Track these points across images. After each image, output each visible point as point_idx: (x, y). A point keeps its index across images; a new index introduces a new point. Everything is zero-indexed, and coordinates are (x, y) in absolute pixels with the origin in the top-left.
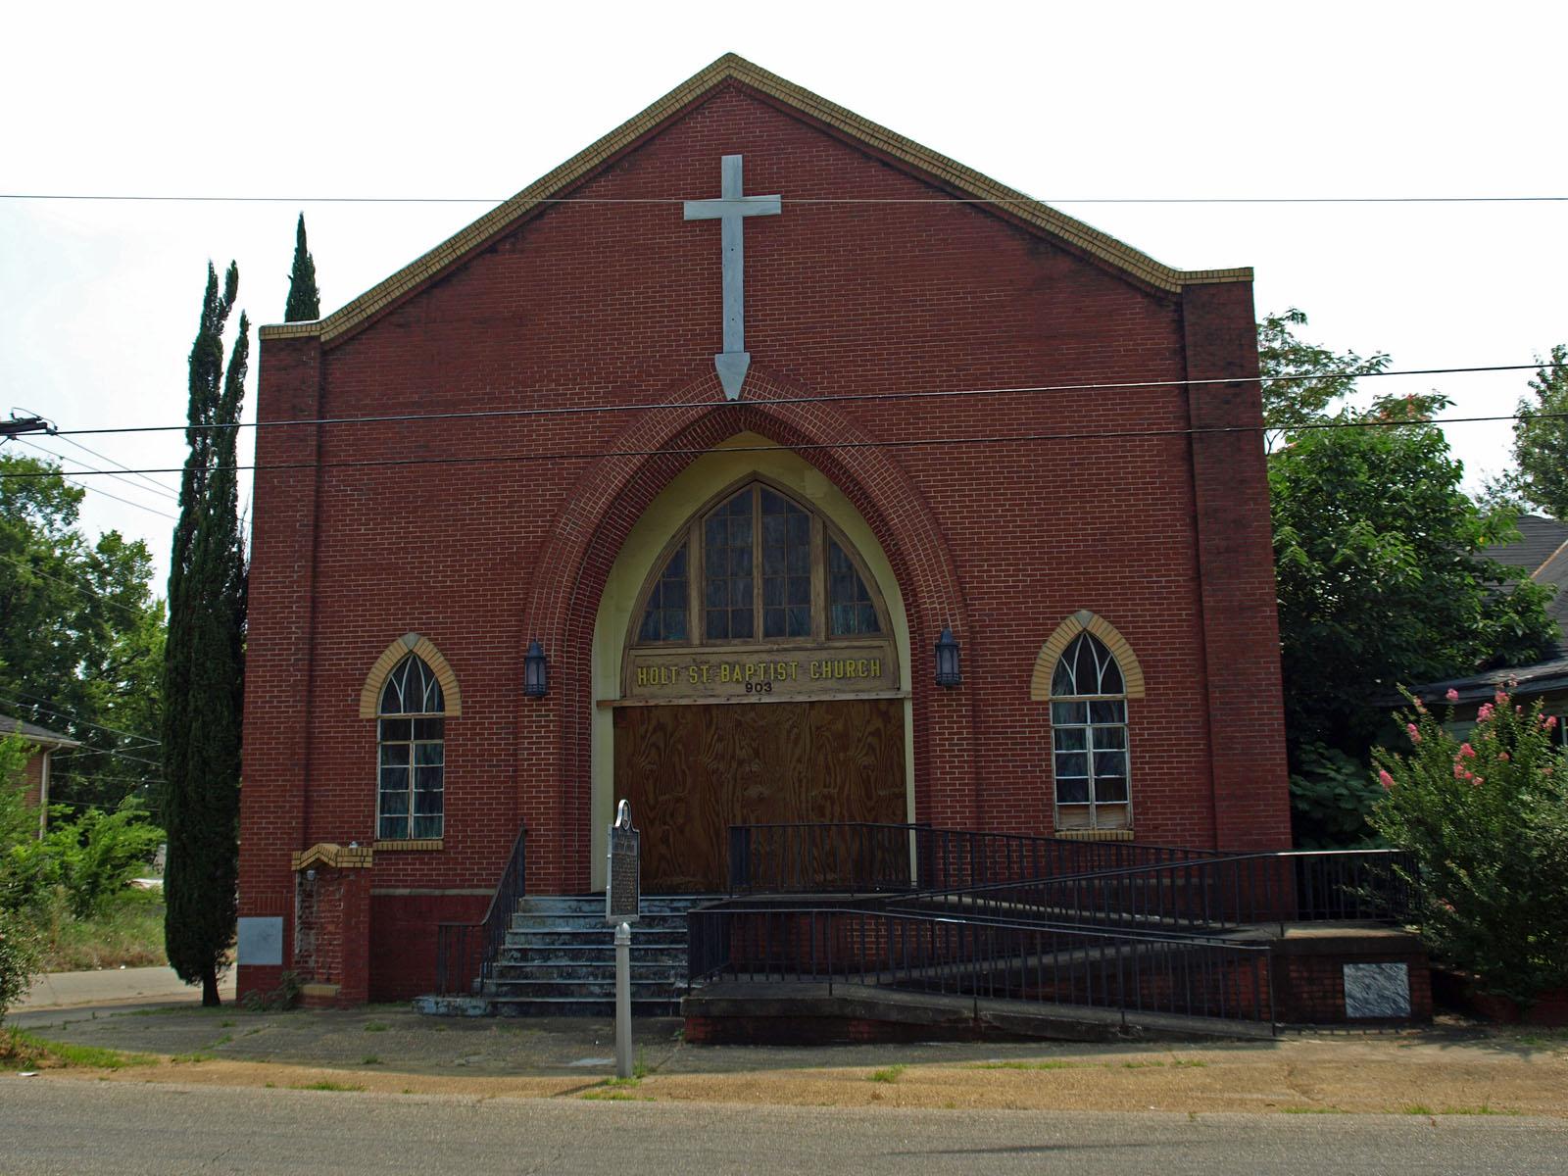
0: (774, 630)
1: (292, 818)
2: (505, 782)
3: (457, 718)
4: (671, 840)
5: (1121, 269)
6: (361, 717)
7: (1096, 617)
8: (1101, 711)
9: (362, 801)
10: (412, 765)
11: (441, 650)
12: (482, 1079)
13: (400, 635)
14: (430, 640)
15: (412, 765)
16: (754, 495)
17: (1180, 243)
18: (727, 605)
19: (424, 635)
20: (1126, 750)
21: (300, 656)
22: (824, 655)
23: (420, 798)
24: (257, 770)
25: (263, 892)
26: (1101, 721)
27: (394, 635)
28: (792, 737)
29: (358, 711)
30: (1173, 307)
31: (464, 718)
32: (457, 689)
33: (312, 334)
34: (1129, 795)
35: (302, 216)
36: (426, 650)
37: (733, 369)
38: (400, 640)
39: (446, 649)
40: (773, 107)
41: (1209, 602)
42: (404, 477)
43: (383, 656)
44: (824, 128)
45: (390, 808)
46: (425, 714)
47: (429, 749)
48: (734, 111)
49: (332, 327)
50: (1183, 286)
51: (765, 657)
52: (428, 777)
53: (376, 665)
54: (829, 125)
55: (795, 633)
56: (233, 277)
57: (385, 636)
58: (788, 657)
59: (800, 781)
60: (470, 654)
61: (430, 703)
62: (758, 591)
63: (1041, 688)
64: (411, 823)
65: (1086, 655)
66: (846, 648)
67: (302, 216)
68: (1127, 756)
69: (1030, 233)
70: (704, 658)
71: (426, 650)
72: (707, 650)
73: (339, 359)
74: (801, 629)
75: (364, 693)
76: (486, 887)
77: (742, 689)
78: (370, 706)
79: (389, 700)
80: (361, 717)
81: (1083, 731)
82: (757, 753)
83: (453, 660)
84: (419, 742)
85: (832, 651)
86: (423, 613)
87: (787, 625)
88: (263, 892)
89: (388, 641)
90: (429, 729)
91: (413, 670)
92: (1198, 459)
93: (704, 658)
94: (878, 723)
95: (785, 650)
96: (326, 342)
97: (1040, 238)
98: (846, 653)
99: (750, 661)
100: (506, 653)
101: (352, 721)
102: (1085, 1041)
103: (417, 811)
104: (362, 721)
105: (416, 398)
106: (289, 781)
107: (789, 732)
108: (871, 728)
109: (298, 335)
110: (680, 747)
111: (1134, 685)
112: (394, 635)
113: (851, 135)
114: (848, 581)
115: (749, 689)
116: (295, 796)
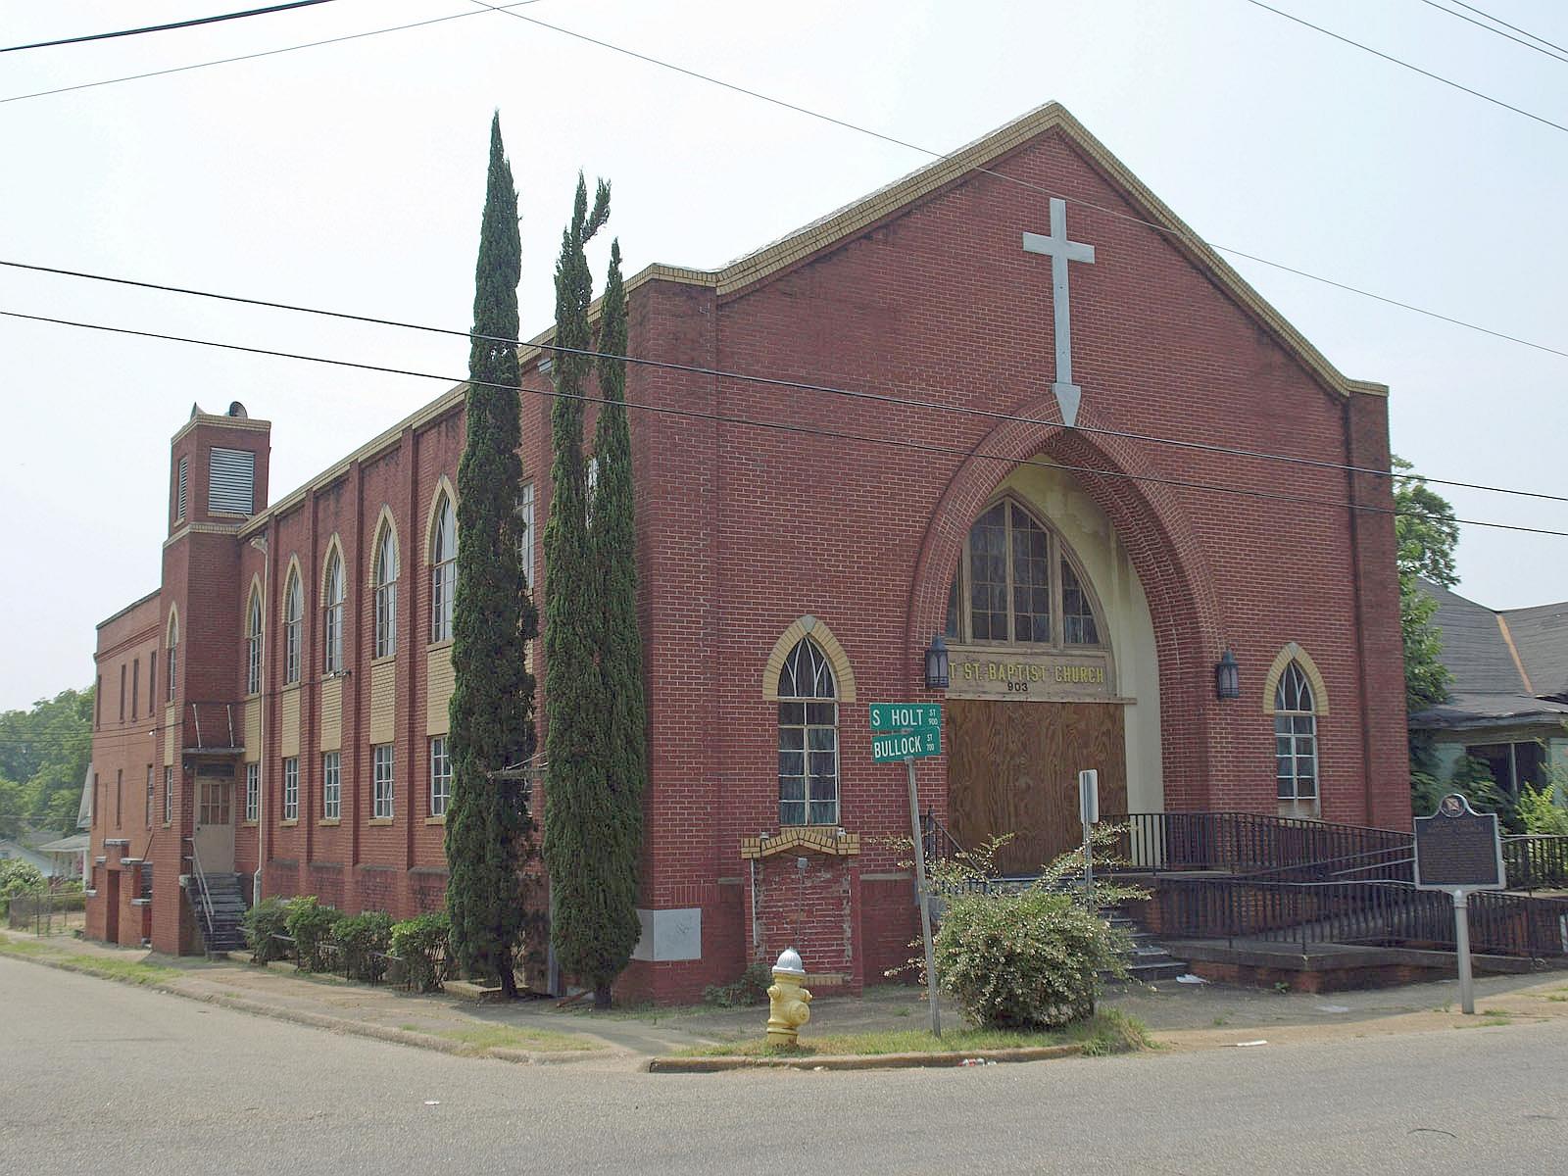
0: (1023, 635)
1: (706, 803)
2: (896, 769)
3: (1326, 717)
4: (961, 827)
5: (1315, 370)
6: (765, 698)
7: (821, 622)
8: (1301, 724)
9: (768, 786)
10: (806, 751)
11: (836, 635)
12: (1381, 1020)
13: (799, 617)
14: (827, 624)
15: (806, 751)
16: (1006, 508)
17: (1351, 360)
18: (987, 609)
19: (820, 618)
20: (1315, 755)
21: (709, 631)
22: (1062, 660)
23: (815, 782)
24: (668, 751)
25: (679, 883)
26: (1300, 732)
27: (793, 616)
28: (1049, 735)
29: (761, 692)
30: (1340, 407)
31: (859, 705)
32: (852, 676)
33: (708, 284)
34: (1317, 791)
35: (497, 114)
36: (824, 635)
37: (1069, 399)
38: (798, 622)
39: (842, 635)
40: (1086, 162)
41: (1367, 644)
42: (796, 454)
43: (782, 636)
44: (1125, 194)
45: (787, 792)
46: (817, 699)
47: (821, 733)
48: (1050, 158)
49: (728, 281)
50: (1351, 392)
51: (1021, 659)
52: (823, 762)
53: (777, 645)
54: (1130, 193)
55: (1038, 640)
56: (604, 197)
57: (784, 616)
58: (1038, 660)
59: (1056, 772)
60: (863, 641)
61: (820, 689)
62: (1010, 598)
63: (1269, 706)
64: (807, 807)
65: (1293, 674)
66: (1081, 656)
67: (497, 114)
68: (1316, 761)
69: (1259, 326)
70: (975, 656)
71: (824, 635)
72: (977, 649)
73: (728, 317)
74: (1042, 636)
75: (766, 673)
76: (883, 872)
77: (1004, 688)
78: (770, 691)
79: (784, 685)
80: (765, 698)
81: (1289, 739)
82: (1024, 746)
83: (847, 646)
84: (813, 727)
85: (1069, 658)
86: (819, 596)
87: (1032, 631)
88: (679, 883)
89: (787, 622)
90: (820, 713)
91: (806, 654)
92: (1361, 534)
93: (975, 656)
94: (1108, 725)
95: (1036, 654)
96: (722, 295)
97: (1265, 332)
98: (1077, 661)
99: (1011, 661)
100: (894, 643)
101: (755, 703)
102: (1504, 973)
103: (813, 796)
104: (765, 702)
105: (803, 373)
106: (702, 763)
107: (1047, 729)
108: (1104, 729)
109: (693, 282)
110: (967, 738)
111: (1321, 705)
112: (793, 616)
113: (1145, 207)
114: (1076, 601)
115: (1010, 686)
116: (709, 780)
